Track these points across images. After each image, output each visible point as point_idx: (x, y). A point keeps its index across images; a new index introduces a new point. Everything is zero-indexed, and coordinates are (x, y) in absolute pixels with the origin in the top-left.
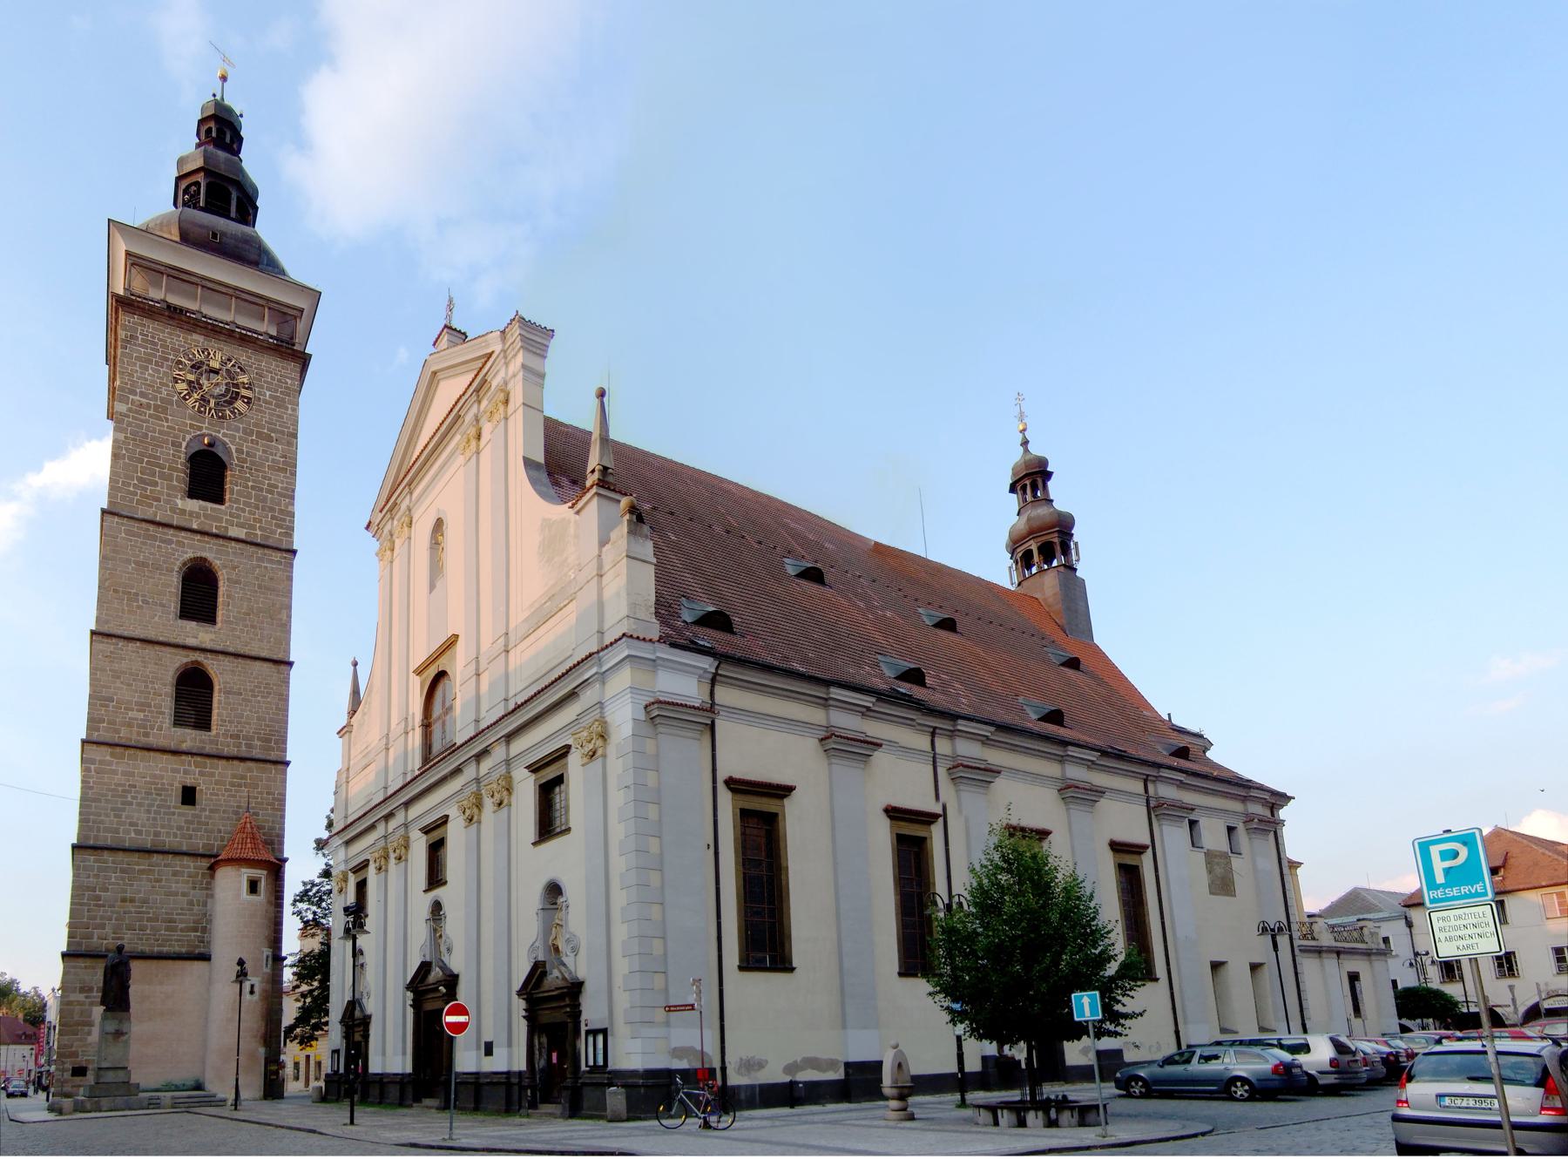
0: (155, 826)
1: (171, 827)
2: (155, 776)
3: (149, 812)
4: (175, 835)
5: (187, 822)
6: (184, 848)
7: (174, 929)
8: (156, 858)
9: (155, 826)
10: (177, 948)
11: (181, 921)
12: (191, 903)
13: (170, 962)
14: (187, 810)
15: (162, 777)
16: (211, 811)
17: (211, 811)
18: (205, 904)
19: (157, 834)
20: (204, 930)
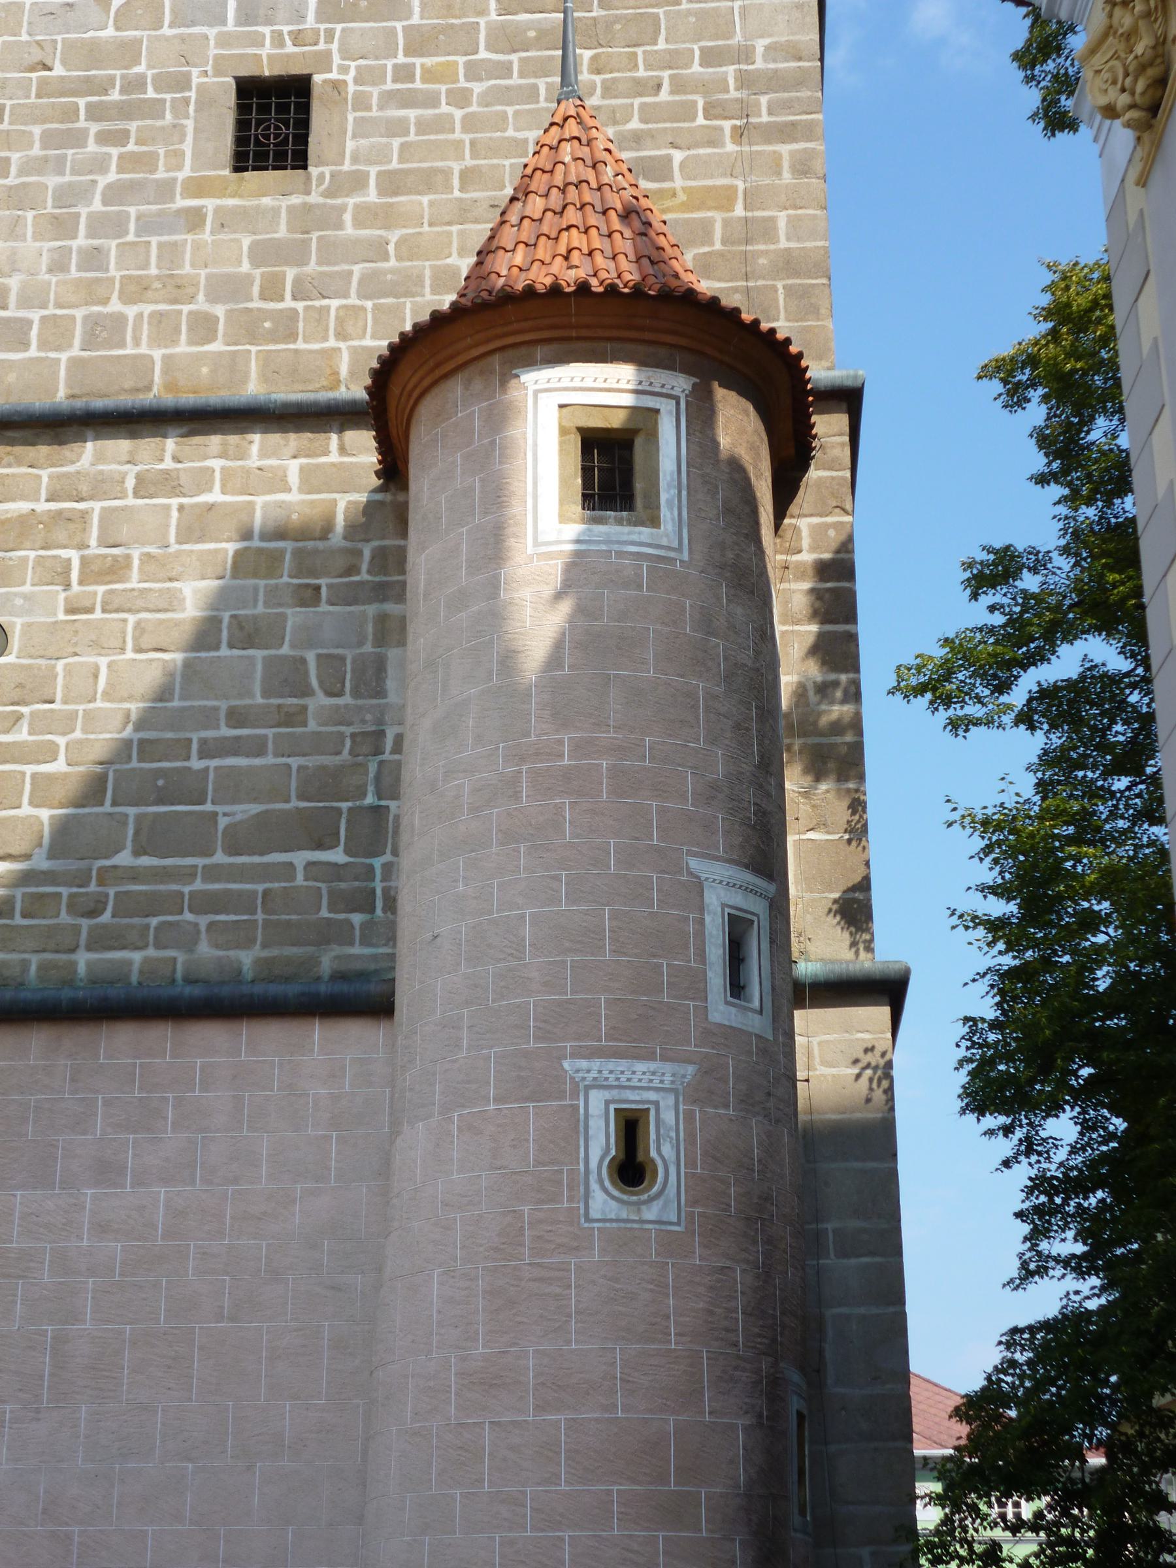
0: (93, 292)
1: (179, 290)
2: (94, 54)
3: (63, 226)
4: (204, 327)
5: (259, 255)
6: (254, 388)
7: (197, 838)
8: (90, 456)
9: (93, 292)
10: (208, 952)
11: (234, 787)
12: (289, 679)
13: (161, 1034)
14: (269, 192)
15: (129, 52)
16: (392, 183)
17: (392, 183)
18: (372, 679)
19: (105, 331)
20: (376, 830)
